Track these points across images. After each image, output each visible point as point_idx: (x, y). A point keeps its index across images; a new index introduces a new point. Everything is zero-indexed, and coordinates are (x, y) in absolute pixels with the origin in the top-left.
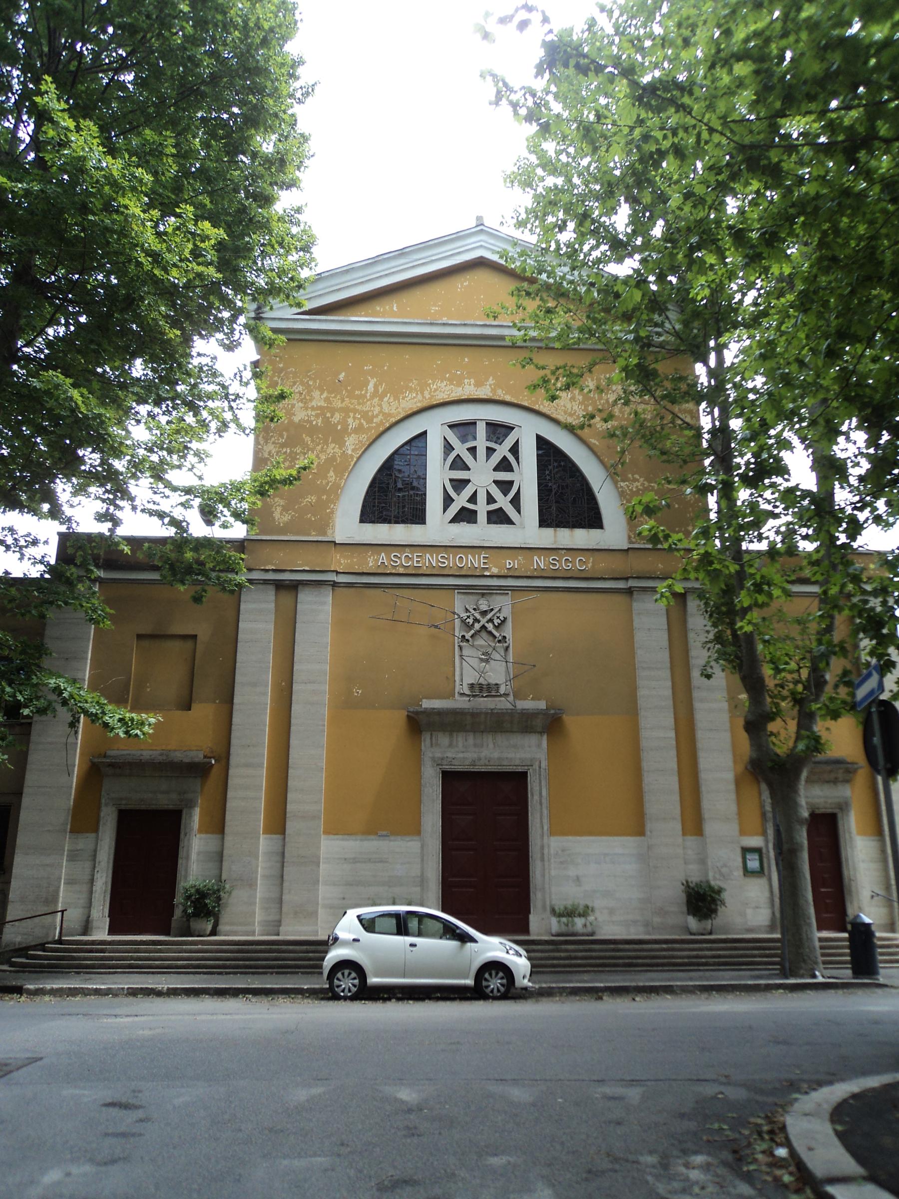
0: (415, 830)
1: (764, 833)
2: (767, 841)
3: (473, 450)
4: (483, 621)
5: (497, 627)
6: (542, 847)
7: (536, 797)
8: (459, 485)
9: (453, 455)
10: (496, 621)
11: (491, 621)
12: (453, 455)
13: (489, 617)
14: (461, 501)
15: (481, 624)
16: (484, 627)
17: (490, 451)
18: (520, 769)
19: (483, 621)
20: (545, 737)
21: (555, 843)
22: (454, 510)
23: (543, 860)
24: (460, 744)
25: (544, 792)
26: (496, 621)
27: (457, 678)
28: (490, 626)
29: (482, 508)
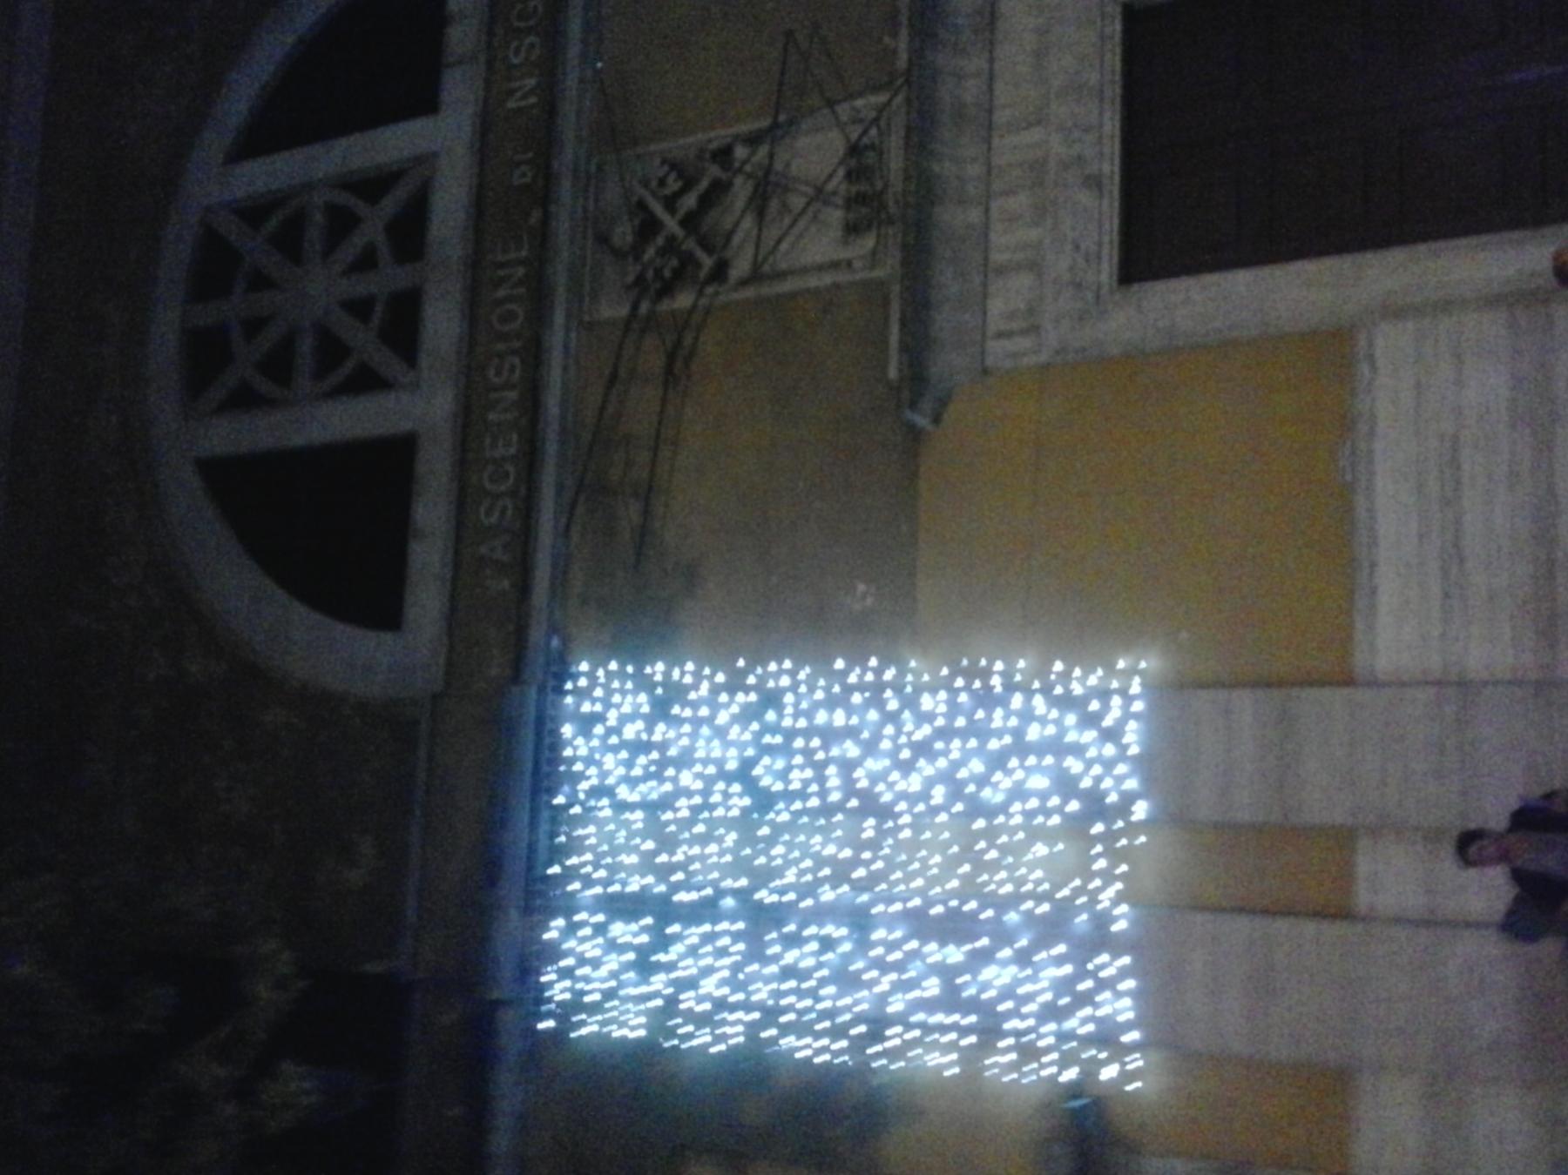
3: (254, 326)
4: (671, 224)
8: (331, 350)
9: (264, 386)
10: (673, 185)
11: (670, 204)
12: (264, 386)
13: (658, 209)
14: (363, 340)
16: (690, 222)
17: (259, 282)
19: (671, 224)
22: (384, 360)
24: (1034, 234)
26: (673, 185)
27: (827, 279)
28: (690, 201)
29: (390, 278)
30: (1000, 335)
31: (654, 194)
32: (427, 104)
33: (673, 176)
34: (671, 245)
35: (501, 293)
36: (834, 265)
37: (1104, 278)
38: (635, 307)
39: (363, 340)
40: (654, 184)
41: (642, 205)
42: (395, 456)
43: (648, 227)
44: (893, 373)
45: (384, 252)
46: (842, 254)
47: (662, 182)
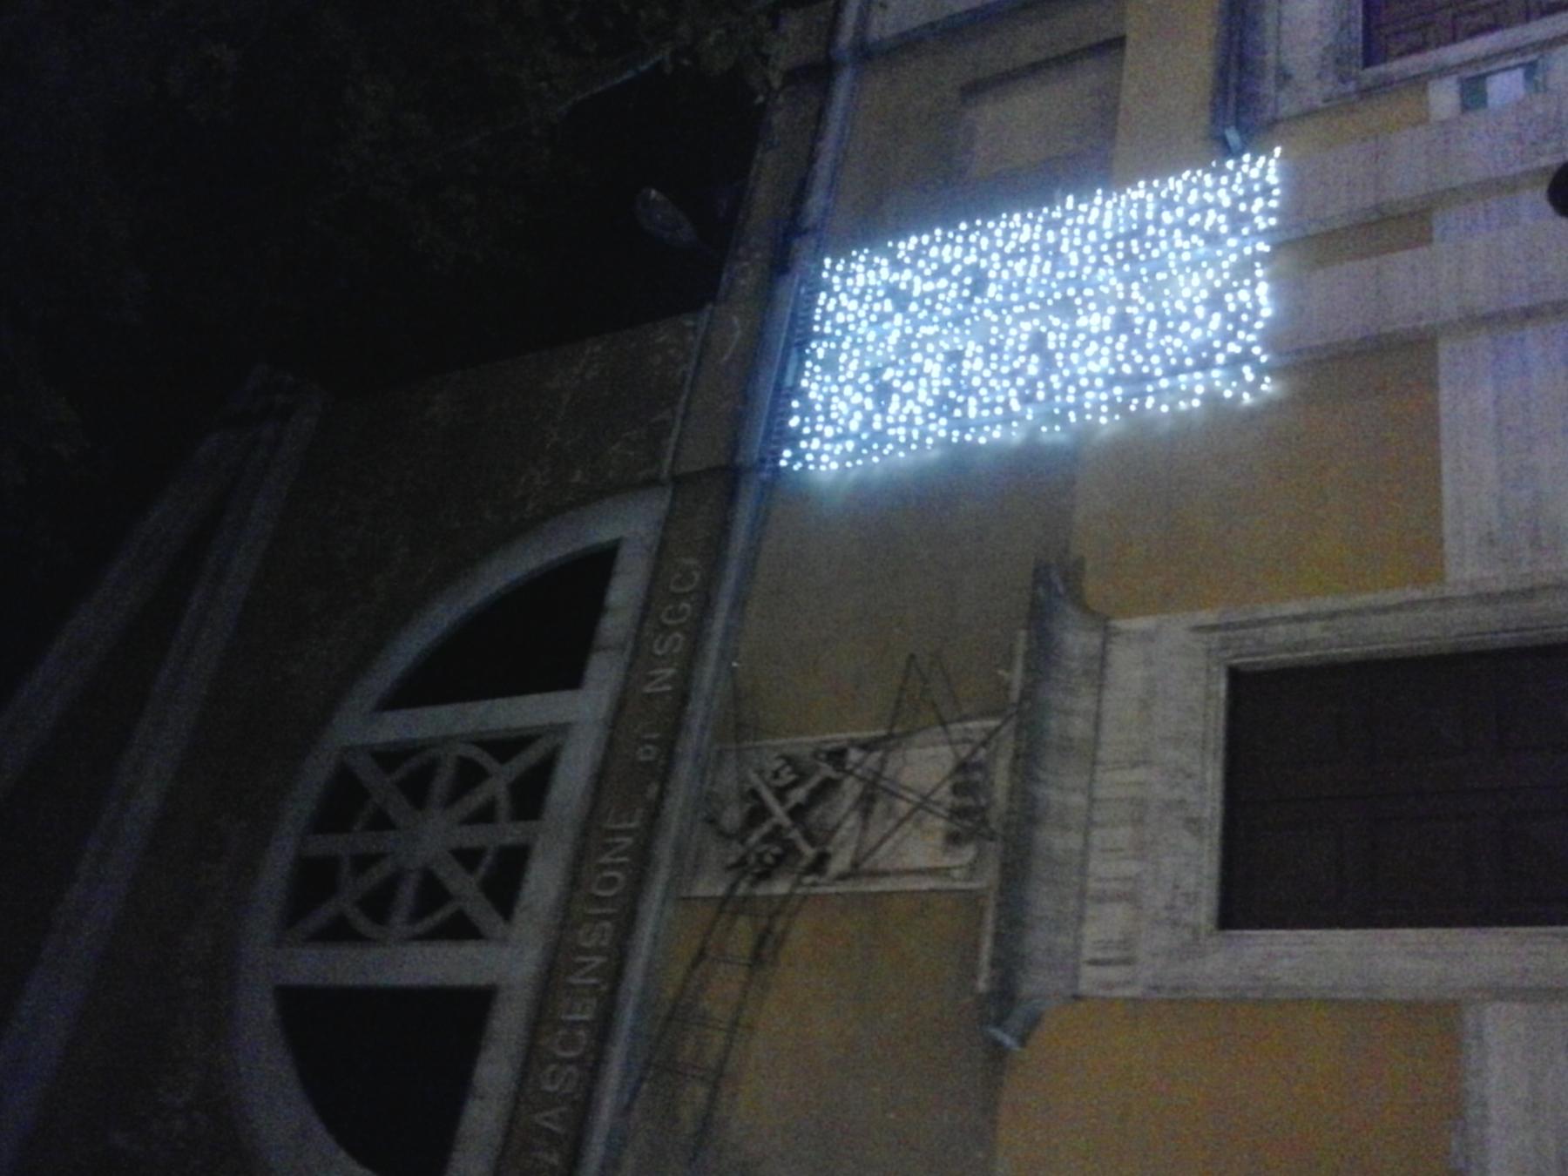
0: (1437, 1024)
1: (1419, 82)
2: (1443, 71)
3: (363, 863)
4: (779, 813)
5: (802, 777)
6: (1488, 598)
7: (1314, 630)
8: (432, 893)
9: (362, 924)
10: (787, 777)
11: (781, 794)
12: (362, 924)
13: (768, 797)
14: (465, 888)
15: (787, 822)
16: (797, 813)
18: (1222, 686)
19: (779, 813)
20: (1121, 624)
21: (1467, 567)
23: (1529, 593)
24: (1132, 868)
25: (1295, 607)
26: (787, 777)
27: (927, 884)
28: (799, 795)
30: (1095, 963)
31: (769, 786)
32: (571, 678)
33: (788, 769)
34: (776, 835)
35: (606, 859)
36: (932, 872)
37: (1203, 919)
38: (734, 887)
39: (465, 888)
40: (768, 776)
41: (754, 794)
42: (473, 1006)
43: (758, 813)
44: (982, 985)
45: (504, 804)
46: (946, 861)
47: (776, 775)
